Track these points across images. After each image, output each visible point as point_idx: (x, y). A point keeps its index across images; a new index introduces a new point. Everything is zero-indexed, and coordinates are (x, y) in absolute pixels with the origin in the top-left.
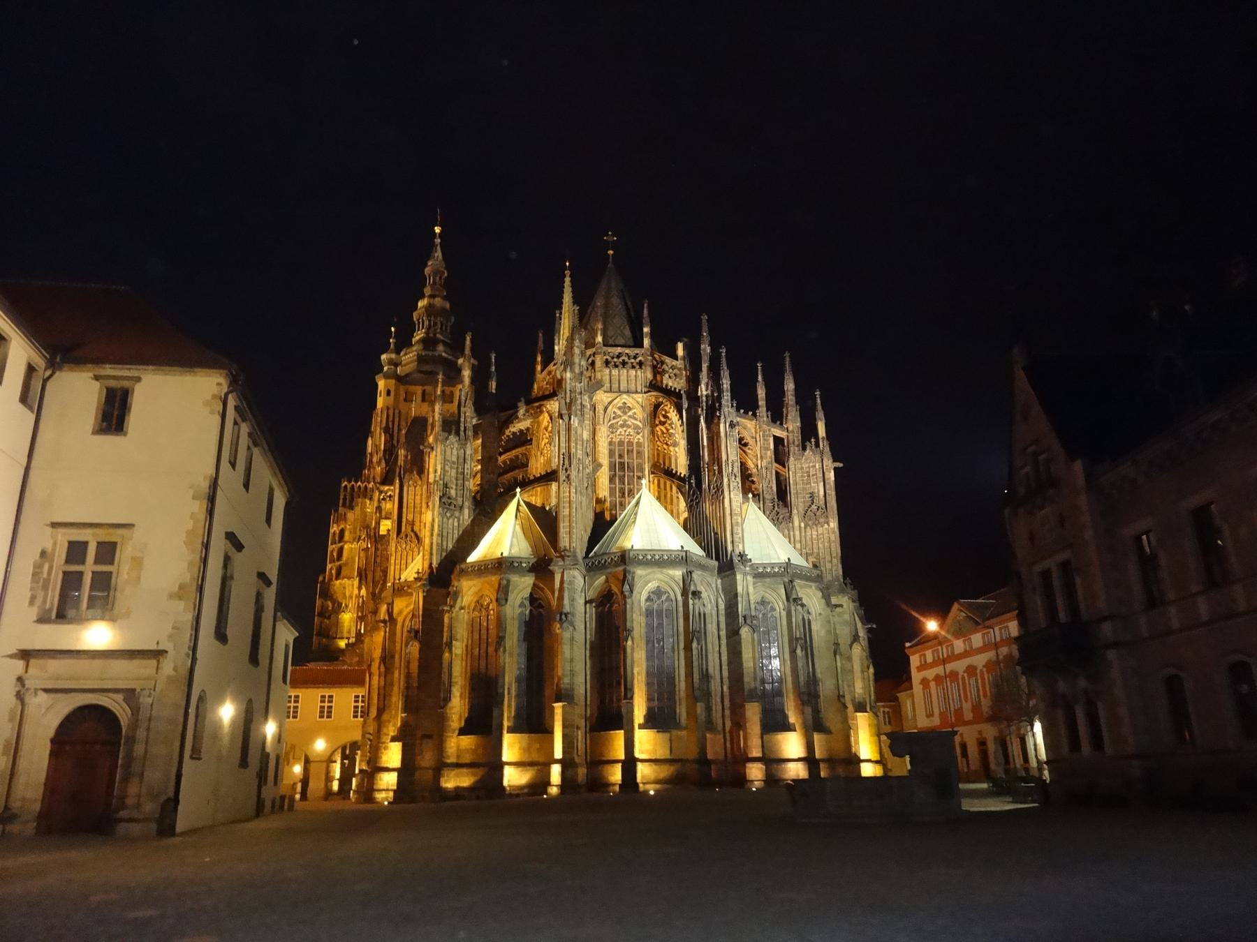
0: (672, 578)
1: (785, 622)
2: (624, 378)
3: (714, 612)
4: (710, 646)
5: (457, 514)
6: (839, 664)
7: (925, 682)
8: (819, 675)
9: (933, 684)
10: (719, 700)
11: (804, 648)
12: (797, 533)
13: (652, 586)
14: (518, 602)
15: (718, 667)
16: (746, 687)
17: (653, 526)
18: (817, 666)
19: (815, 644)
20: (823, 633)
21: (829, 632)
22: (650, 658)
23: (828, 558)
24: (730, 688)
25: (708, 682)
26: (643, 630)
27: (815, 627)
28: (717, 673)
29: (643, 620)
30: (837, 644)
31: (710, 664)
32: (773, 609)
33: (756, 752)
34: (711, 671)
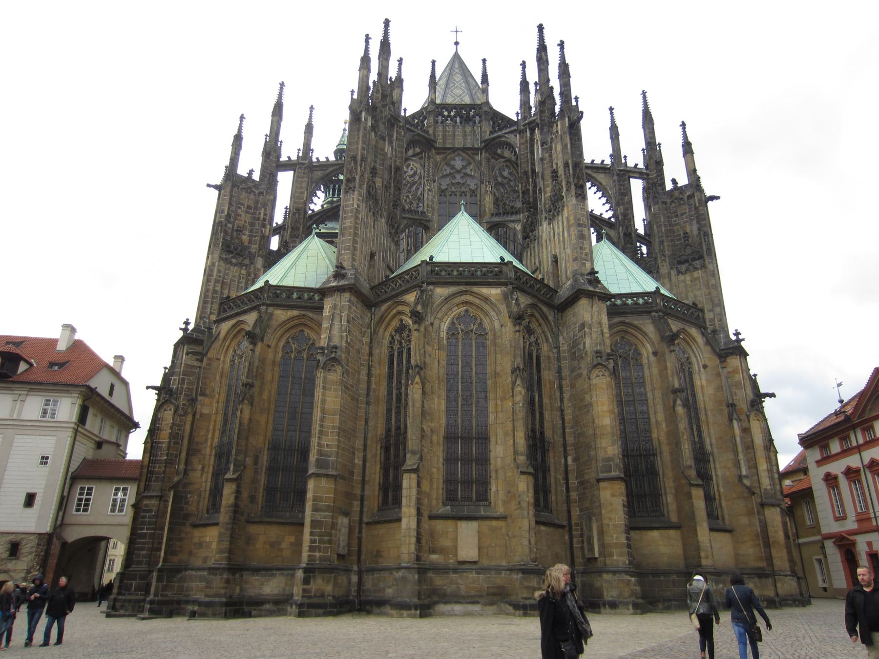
0: (486, 299)
1: (655, 371)
2: (459, 131)
3: (553, 355)
4: (546, 400)
5: (247, 262)
6: (737, 431)
7: (831, 480)
8: (708, 448)
9: (843, 482)
10: (560, 477)
11: (686, 405)
12: (666, 281)
13: (457, 311)
14: (281, 344)
15: (560, 431)
16: (601, 455)
17: (464, 241)
18: (705, 433)
19: (701, 405)
20: (710, 391)
21: (720, 388)
22: (450, 411)
23: (710, 307)
24: (576, 460)
25: (544, 453)
26: (443, 371)
27: (697, 383)
28: (559, 439)
29: (443, 355)
30: (733, 405)
31: (546, 425)
32: (639, 354)
33: (619, 559)
34: (548, 433)
